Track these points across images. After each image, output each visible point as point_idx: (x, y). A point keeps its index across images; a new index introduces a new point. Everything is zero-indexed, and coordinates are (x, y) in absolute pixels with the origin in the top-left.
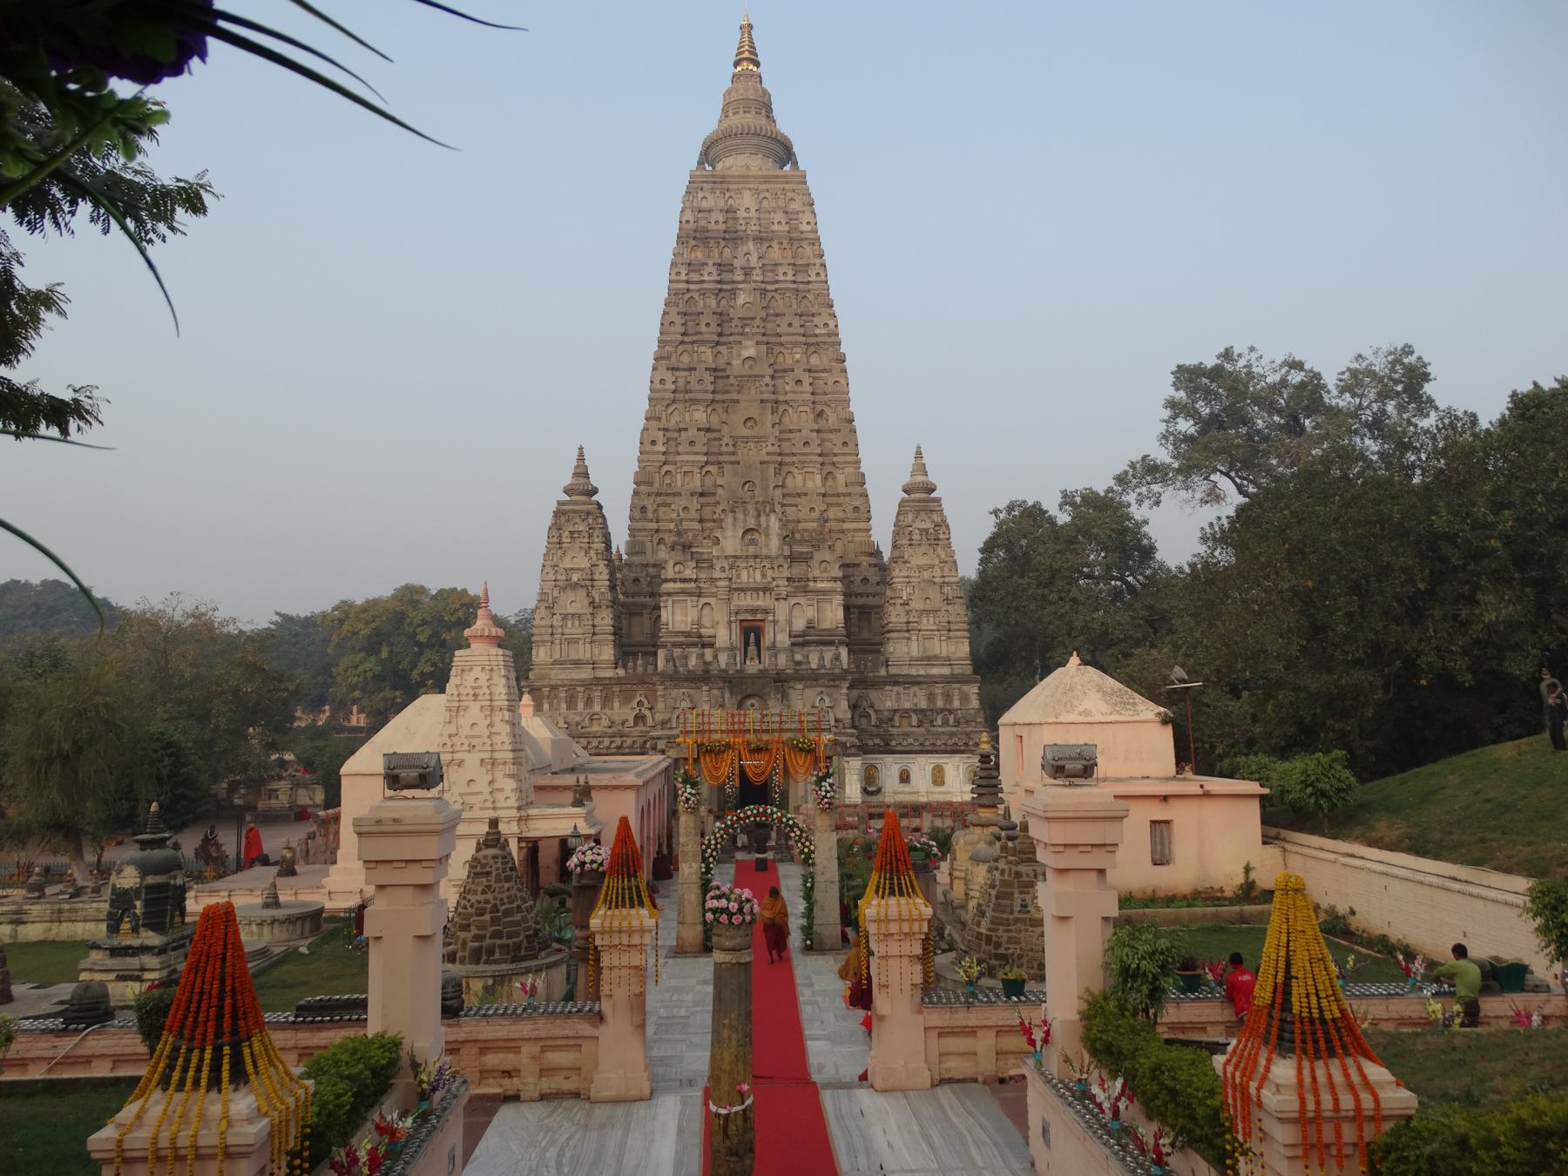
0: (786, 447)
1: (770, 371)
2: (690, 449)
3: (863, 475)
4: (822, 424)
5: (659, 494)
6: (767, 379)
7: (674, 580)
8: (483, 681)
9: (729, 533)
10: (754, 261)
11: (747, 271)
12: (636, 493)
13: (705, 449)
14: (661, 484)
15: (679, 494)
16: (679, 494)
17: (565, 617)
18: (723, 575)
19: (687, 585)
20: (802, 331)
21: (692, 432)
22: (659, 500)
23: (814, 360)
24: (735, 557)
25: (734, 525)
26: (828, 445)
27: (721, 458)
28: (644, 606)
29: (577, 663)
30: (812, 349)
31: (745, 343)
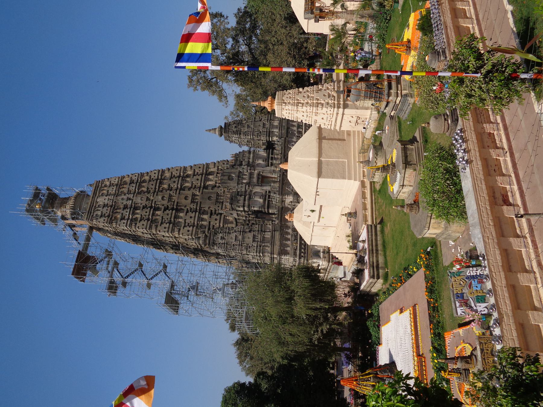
2: (193, 218)
3: (212, 163)
6: (171, 192)
9: (228, 185)
10: (125, 197)
11: (129, 199)
15: (210, 222)
16: (210, 222)
17: (254, 241)
25: (225, 183)
29: (273, 237)
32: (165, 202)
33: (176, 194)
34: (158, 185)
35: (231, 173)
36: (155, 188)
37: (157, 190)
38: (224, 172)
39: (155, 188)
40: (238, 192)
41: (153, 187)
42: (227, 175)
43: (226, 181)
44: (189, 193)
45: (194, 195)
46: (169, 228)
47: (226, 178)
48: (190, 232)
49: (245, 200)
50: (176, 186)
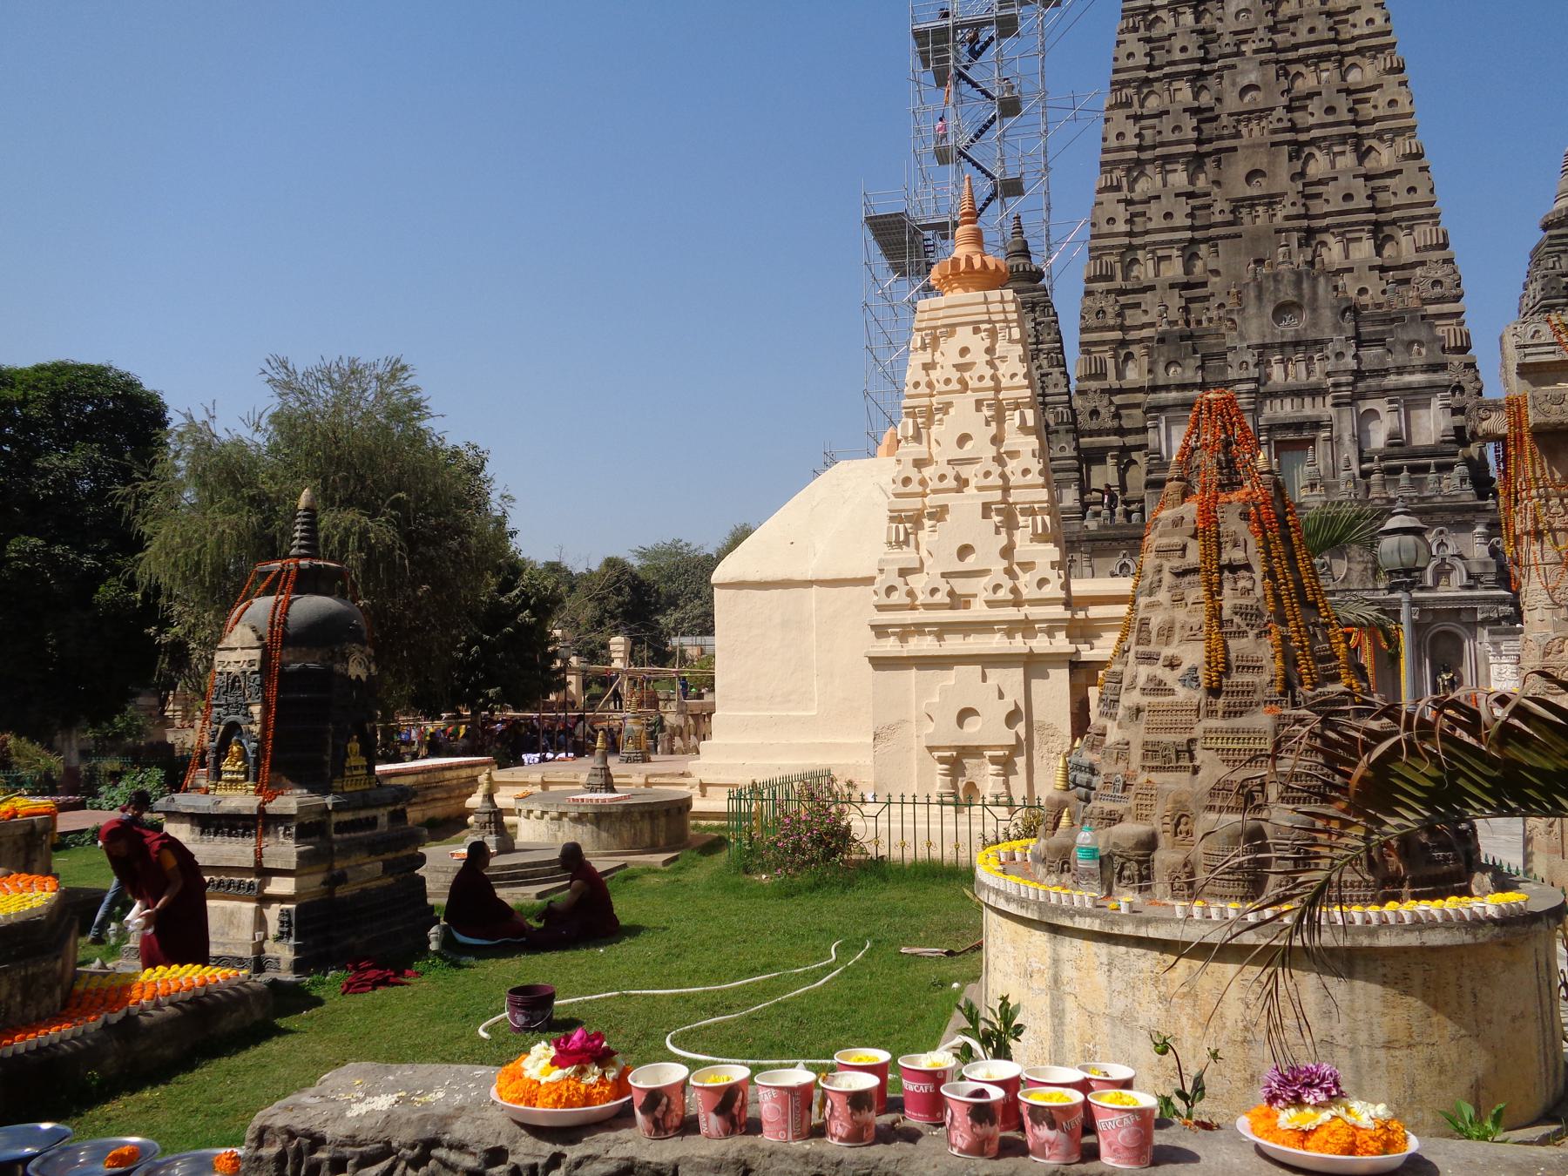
0: (1317, 207)
1: (1284, 100)
4: (1370, 164)
5: (1122, 292)
7: (1167, 388)
8: (978, 356)
9: (1252, 310)
12: (1088, 293)
13: (1188, 222)
14: (1126, 278)
15: (1152, 288)
16: (1152, 288)
18: (1245, 376)
19: (1189, 394)
20: (1332, 35)
21: (1167, 203)
22: (1122, 300)
23: (1354, 77)
24: (1264, 346)
25: (1259, 298)
26: (1383, 198)
27: (1212, 232)
28: (1112, 448)
30: (1348, 61)
31: (1240, 67)
32: (1232, 103)
33: (1275, 132)
34: (1313, 50)
35: (1314, 310)
36: (1296, 47)
37: (1291, 55)
38: (1315, 279)
39: (1296, 47)
40: (1222, 356)
41: (1303, 36)
42: (1301, 296)
43: (1267, 296)
44: (1281, 178)
45: (1271, 200)
46: (1123, 149)
47: (1288, 294)
48: (1105, 229)
49: (1182, 387)
50: (1311, 121)
